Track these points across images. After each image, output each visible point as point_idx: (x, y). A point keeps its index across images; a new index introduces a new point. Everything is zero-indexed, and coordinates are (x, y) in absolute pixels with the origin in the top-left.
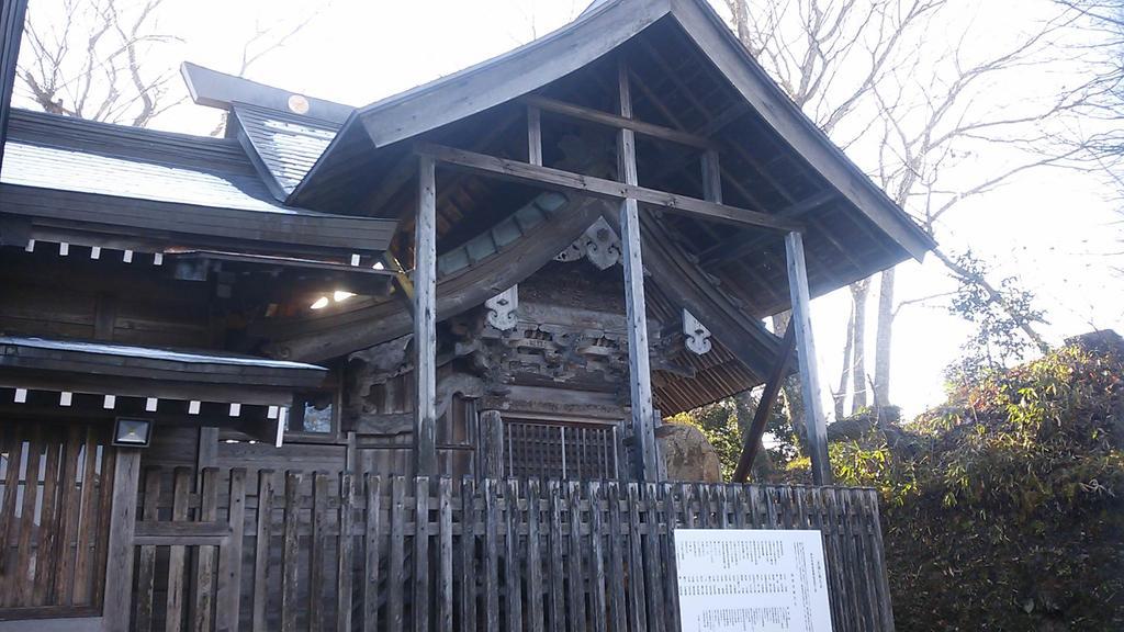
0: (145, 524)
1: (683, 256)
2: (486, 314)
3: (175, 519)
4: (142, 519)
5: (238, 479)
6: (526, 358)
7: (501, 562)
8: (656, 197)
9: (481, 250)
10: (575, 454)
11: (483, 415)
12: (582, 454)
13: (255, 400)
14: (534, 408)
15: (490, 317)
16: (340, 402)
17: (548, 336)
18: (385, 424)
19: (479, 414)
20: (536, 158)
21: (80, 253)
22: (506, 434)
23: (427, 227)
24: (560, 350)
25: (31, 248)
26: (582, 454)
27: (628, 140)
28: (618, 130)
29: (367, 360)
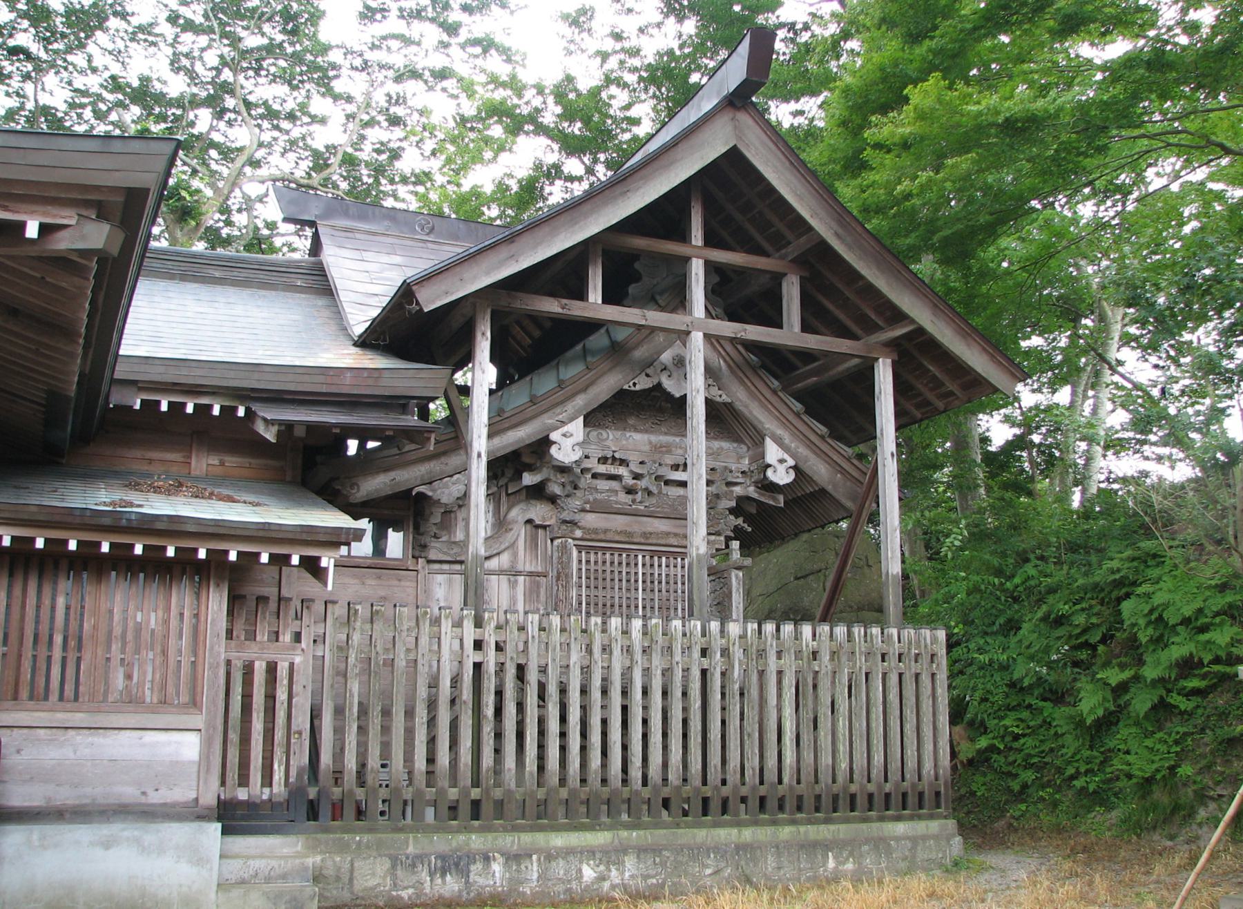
0: (233, 643)
1: (763, 379)
2: (550, 447)
3: (258, 638)
4: (231, 639)
5: (308, 608)
6: (603, 485)
7: (542, 687)
8: (728, 328)
9: (545, 382)
10: (652, 582)
11: (557, 542)
12: (660, 582)
13: (311, 552)
14: (609, 536)
15: (553, 450)
16: (411, 530)
17: (623, 462)
18: (454, 551)
19: (552, 540)
20: (595, 295)
21: (177, 408)
22: (580, 561)
23: (480, 372)
24: (637, 477)
25: (137, 407)
26: (660, 582)
27: (697, 269)
28: (687, 260)
29: (430, 494)
